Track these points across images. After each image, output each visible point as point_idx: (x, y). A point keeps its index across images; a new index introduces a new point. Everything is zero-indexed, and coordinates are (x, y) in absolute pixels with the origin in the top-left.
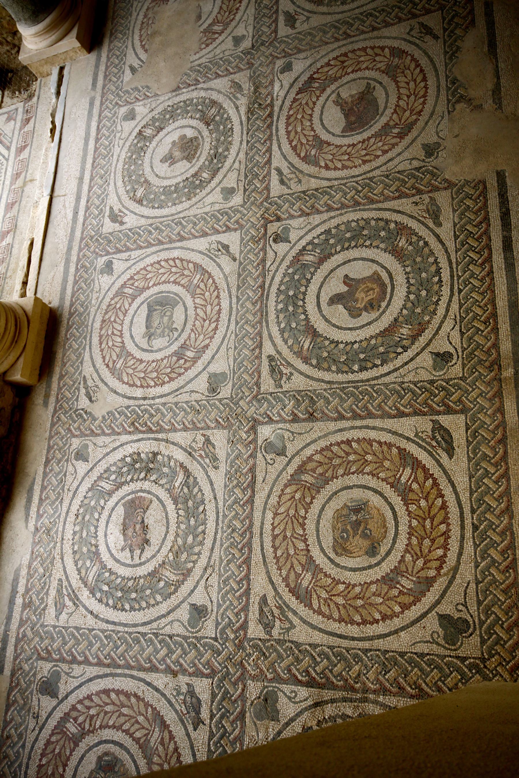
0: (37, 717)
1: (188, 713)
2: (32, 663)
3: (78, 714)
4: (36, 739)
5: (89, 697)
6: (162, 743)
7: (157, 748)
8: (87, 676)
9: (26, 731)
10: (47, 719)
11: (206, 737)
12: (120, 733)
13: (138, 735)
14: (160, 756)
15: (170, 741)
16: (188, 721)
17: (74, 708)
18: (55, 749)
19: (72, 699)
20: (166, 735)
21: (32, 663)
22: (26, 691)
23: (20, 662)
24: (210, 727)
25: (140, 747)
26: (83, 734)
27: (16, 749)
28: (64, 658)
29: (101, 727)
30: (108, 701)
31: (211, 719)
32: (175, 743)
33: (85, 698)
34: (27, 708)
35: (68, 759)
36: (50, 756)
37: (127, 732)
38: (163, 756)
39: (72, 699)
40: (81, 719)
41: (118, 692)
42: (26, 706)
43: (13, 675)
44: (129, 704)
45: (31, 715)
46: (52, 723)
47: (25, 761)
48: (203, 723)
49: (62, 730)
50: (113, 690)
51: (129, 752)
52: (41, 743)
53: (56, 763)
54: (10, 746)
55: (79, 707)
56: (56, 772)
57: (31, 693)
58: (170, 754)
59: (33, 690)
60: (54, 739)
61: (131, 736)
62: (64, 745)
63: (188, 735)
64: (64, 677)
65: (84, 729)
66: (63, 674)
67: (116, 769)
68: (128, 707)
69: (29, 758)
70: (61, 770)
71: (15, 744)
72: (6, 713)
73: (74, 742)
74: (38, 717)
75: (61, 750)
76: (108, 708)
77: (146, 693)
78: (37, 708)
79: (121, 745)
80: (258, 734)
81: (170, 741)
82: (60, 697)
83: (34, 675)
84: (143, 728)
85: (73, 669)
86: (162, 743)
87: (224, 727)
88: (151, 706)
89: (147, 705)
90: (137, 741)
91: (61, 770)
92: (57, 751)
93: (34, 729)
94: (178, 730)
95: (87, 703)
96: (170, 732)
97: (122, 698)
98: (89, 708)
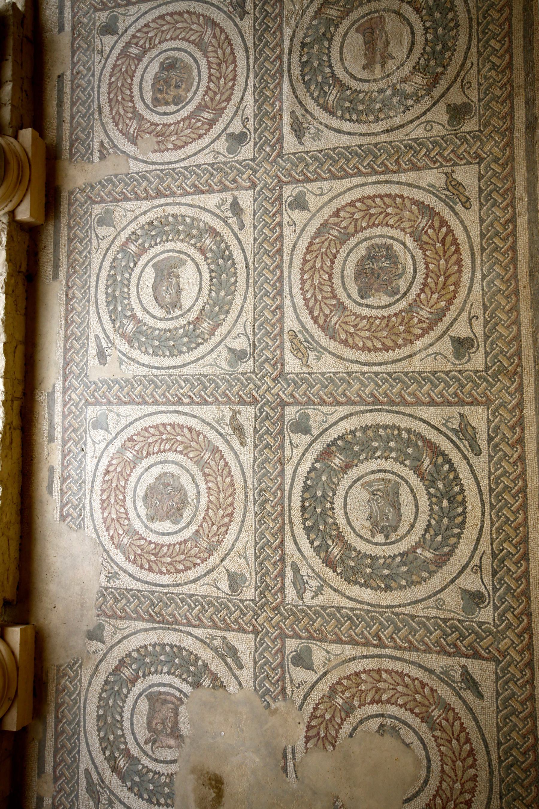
0: (101, 52)
1: (235, 10)
2: (91, 16)
3: (138, 40)
4: (104, 67)
5: (147, 25)
6: (215, 36)
7: (210, 42)
8: (142, 11)
9: (94, 65)
10: (111, 51)
11: (252, 22)
12: (177, 41)
13: (193, 38)
14: (213, 46)
15: (221, 34)
16: (235, 16)
17: (134, 36)
18: (121, 69)
19: (131, 31)
20: (218, 31)
21: (91, 16)
22: (88, 36)
23: (78, 19)
24: (254, 14)
25: (196, 46)
26: (145, 52)
27: (86, 79)
28: (119, 4)
29: (159, 43)
30: (163, 23)
31: (255, 8)
32: (226, 33)
33: (142, 27)
34: (91, 49)
35: (134, 72)
36: (118, 75)
37: (183, 39)
38: (217, 46)
39: (131, 31)
40: (141, 43)
41: (171, 14)
42: (91, 48)
43: (73, 28)
44: (183, 20)
45: (96, 52)
46: (116, 52)
47: (96, 84)
48: (248, 13)
49: (126, 55)
50: (168, 14)
51: (186, 51)
52: (109, 68)
53: (124, 77)
54: (81, 78)
55: (138, 34)
56: (125, 83)
57: (94, 37)
58: (222, 42)
59: (94, 35)
60: (119, 62)
61: (187, 40)
62: (129, 64)
63: (236, 25)
64: (121, 18)
65: (145, 48)
66: (120, 16)
67: (177, 66)
68: (182, 22)
69: (100, 81)
70: (129, 81)
71: (85, 76)
72: (73, 57)
73: (138, 60)
74: (102, 52)
75: (127, 68)
76: (164, 28)
77: (197, 7)
78: (100, 46)
79: (179, 49)
80: (295, 7)
81: (221, 34)
82: (120, 33)
83: (94, 24)
84: (197, 32)
85: (128, 10)
86: (215, 36)
87: (266, 10)
88: (203, 15)
89: (198, 16)
90: (193, 42)
91: (129, 81)
92: (123, 69)
93: (100, 61)
94: (228, 25)
95: (145, 30)
96: (221, 28)
97: (176, 17)
98: (147, 33)
